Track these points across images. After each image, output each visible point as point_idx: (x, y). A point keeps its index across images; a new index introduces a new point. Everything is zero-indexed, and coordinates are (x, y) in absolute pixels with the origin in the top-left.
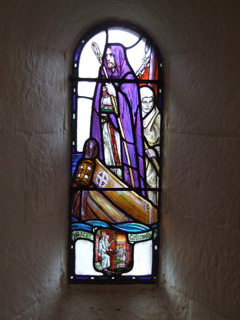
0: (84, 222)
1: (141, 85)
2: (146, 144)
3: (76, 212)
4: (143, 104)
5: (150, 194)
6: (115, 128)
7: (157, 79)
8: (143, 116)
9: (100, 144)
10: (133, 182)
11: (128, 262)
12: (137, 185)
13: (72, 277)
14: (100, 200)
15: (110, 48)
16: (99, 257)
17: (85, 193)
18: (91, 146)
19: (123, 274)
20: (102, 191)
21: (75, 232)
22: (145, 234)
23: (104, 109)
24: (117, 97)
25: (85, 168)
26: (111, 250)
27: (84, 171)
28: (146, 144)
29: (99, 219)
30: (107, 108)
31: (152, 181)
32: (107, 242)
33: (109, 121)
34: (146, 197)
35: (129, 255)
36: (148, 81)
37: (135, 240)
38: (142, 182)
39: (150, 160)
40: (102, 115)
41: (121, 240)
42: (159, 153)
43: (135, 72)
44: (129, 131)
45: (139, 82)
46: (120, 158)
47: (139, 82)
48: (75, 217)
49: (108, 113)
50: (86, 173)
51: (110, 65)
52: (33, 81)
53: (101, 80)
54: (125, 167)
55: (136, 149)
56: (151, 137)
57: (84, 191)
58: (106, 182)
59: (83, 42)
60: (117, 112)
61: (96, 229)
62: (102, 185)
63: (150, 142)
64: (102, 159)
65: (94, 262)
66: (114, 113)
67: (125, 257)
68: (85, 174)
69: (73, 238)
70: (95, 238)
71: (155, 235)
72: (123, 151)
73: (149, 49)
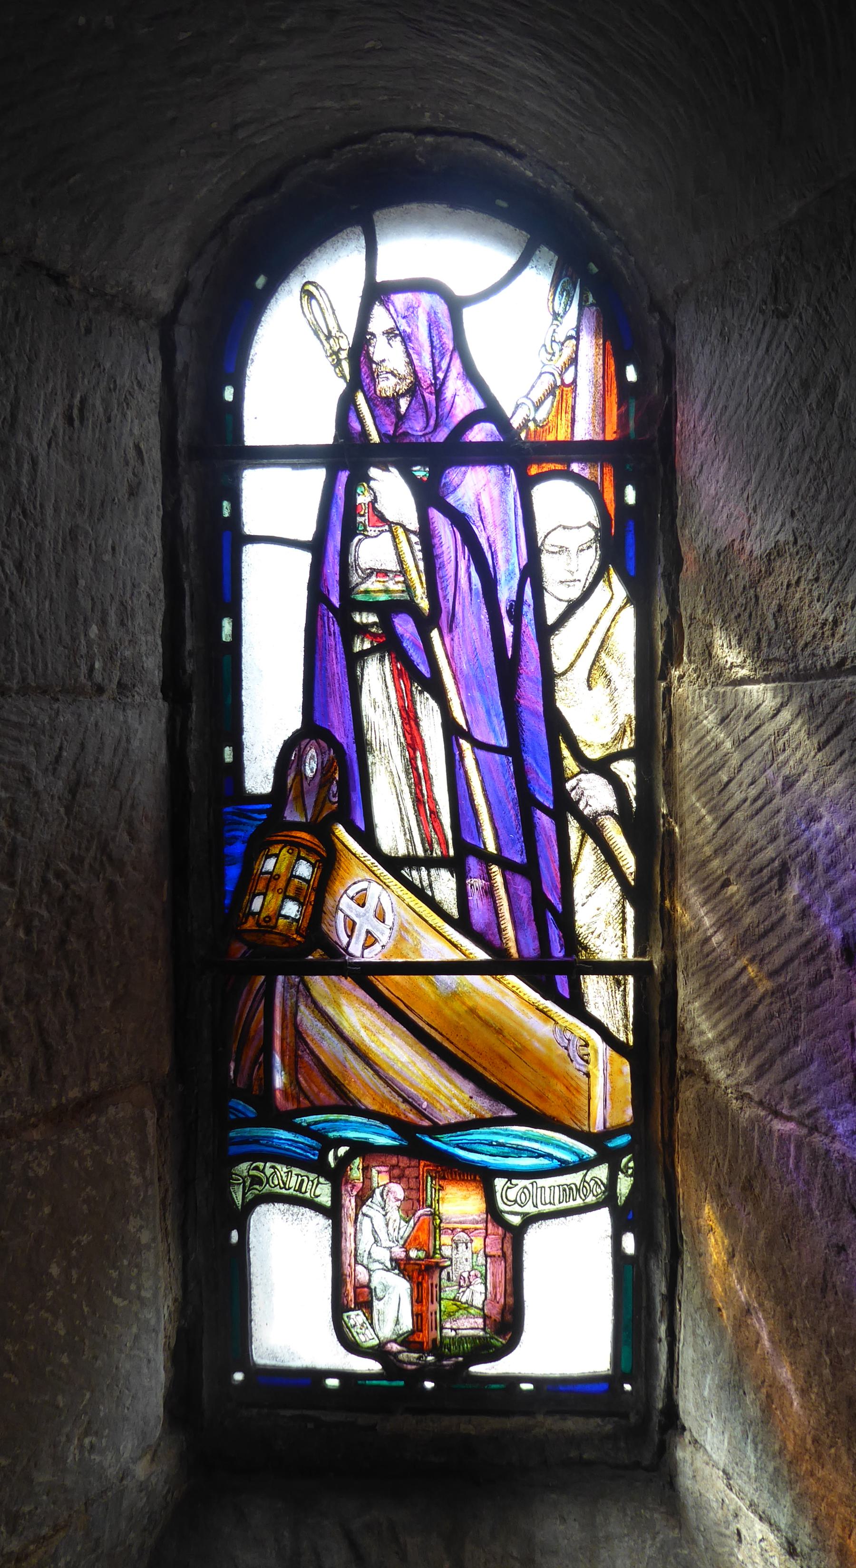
0: (286, 1121)
2: (566, 752)
3: (250, 1075)
5: (597, 992)
6: (418, 678)
7: (610, 436)
8: (551, 619)
10: (510, 932)
11: (494, 1311)
12: (532, 949)
13: (239, 1376)
14: (357, 1016)
15: (385, 304)
16: (358, 1287)
18: (311, 768)
20: (365, 976)
21: (244, 1167)
22: (575, 1178)
23: (367, 592)
24: (426, 534)
25: (283, 869)
27: (281, 884)
28: (566, 752)
30: (379, 586)
33: (389, 645)
34: (575, 1005)
35: (501, 1278)
37: (529, 1209)
38: (554, 933)
39: (592, 828)
41: (460, 1204)
42: (632, 792)
43: (508, 411)
44: (482, 690)
45: (524, 457)
47: (524, 457)
49: (386, 610)
51: (386, 386)
53: (347, 458)
54: (473, 863)
56: (597, 711)
57: (280, 978)
58: (383, 933)
59: (261, 282)
60: (424, 604)
61: (342, 1151)
62: (365, 947)
64: (361, 825)
65: (339, 1308)
66: (408, 606)
68: (286, 897)
70: (336, 1196)
71: (624, 1185)
72: (461, 783)
73: (570, 298)
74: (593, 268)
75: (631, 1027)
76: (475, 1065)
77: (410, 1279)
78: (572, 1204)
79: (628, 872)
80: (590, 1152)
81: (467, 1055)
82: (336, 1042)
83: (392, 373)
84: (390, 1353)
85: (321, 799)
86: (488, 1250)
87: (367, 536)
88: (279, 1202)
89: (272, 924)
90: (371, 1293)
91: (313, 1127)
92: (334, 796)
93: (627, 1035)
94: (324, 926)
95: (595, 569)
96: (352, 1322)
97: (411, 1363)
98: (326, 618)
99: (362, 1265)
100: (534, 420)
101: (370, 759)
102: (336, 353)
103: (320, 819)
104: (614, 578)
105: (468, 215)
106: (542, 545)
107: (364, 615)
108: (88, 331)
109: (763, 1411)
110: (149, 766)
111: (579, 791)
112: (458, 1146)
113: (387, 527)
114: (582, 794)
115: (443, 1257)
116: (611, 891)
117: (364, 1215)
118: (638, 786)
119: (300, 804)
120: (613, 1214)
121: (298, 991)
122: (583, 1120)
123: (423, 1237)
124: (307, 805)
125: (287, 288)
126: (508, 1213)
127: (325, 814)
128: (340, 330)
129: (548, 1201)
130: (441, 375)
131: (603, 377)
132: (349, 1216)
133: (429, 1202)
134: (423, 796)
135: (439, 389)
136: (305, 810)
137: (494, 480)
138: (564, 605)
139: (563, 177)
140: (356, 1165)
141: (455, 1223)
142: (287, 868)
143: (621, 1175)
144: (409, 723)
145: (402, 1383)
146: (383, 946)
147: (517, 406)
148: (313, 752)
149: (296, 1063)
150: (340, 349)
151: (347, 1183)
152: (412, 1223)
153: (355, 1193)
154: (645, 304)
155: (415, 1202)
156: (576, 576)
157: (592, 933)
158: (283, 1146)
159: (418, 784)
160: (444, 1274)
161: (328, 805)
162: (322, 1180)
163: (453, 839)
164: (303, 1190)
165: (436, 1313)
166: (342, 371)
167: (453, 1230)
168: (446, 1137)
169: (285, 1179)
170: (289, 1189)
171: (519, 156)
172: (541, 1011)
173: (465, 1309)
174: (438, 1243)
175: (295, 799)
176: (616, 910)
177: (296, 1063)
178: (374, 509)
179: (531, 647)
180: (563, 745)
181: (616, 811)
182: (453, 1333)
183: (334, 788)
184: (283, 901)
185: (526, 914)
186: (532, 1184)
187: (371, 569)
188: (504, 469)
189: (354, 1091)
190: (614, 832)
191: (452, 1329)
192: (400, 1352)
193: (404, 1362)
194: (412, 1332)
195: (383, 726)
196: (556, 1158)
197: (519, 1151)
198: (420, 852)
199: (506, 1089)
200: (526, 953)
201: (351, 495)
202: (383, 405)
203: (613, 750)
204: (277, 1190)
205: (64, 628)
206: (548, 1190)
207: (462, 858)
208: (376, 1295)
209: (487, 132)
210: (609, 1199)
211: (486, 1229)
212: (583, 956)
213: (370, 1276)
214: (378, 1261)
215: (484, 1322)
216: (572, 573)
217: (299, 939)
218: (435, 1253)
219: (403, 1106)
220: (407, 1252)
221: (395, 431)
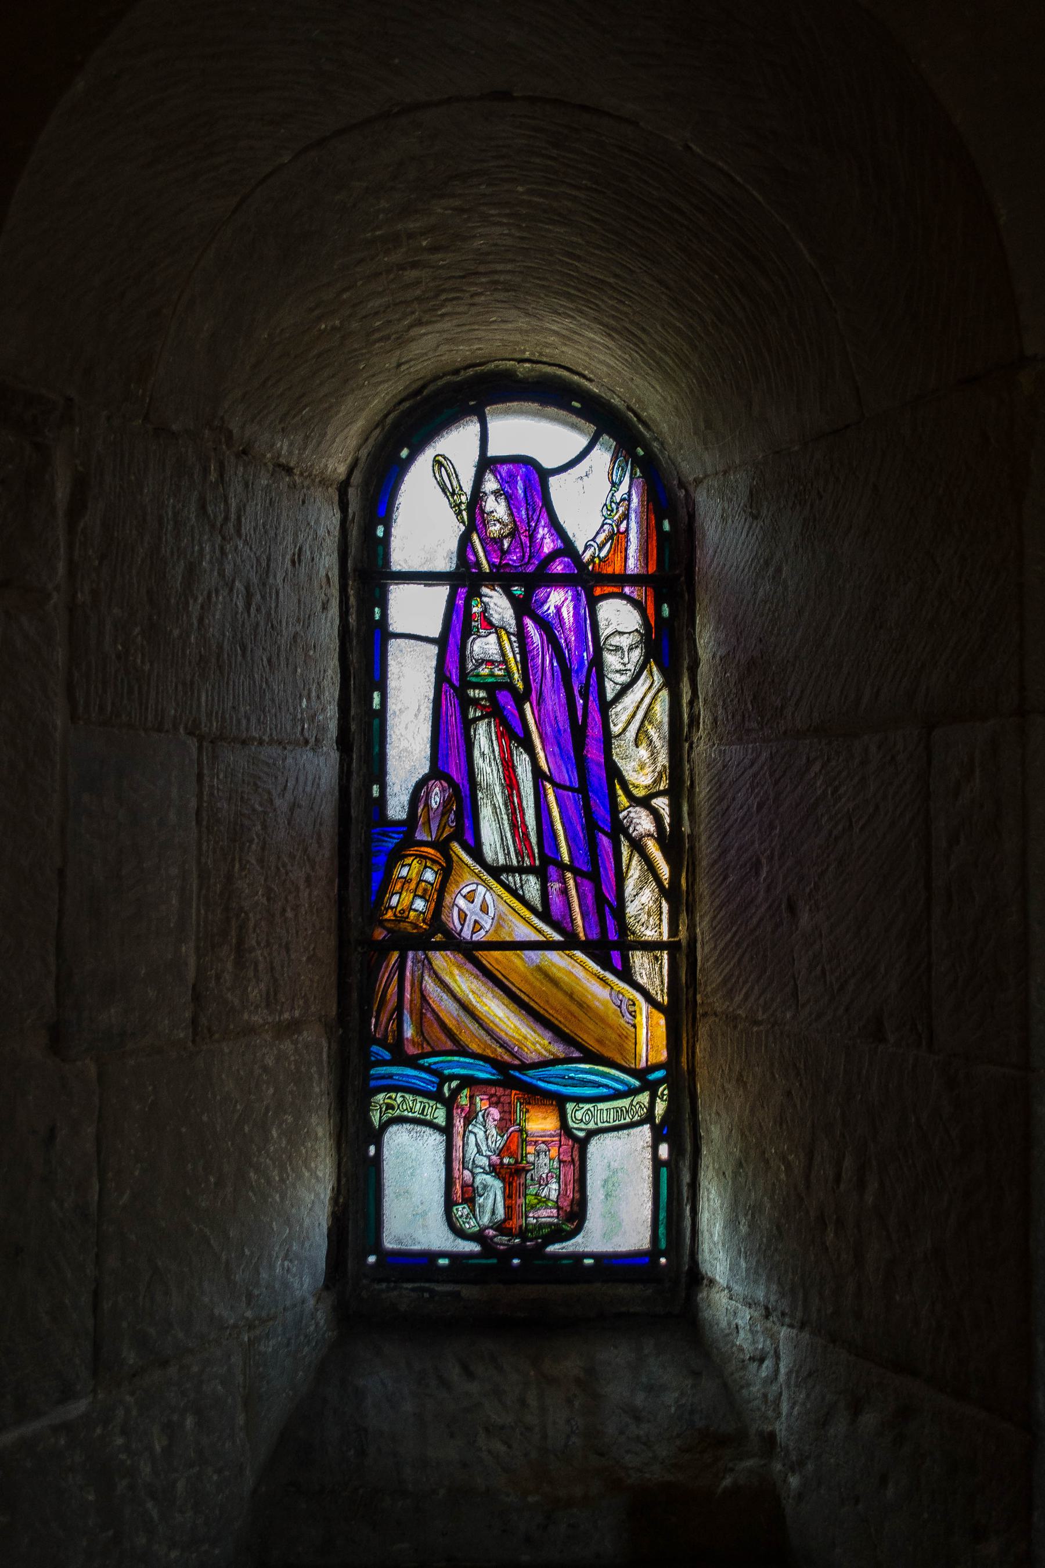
0: (412, 1062)
2: (620, 792)
4: (605, 654)
5: (641, 963)
11: (565, 1204)
13: (372, 1259)
15: (495, 472)
16: (465, 1185)
18: (435, 801)
19: (551, 1249)
20: (470, 952)
21: (380, 1097)
22: (625, 1103)
23: (478, 676)
25: (414, 874)
27: (413, 886)
28: (620, 792)
30: (486, 672)
31: (644, 918)
32: (494, 1132)
33: (494, 712)
34: (626, 974)
35: (570, 1177)
37: (592, 1126)
38: (610, 922)
39: (638, 846)
40: (471, 693)
41: (541, 1123)
42: (667, 820)
43: (581, 549)
45: (590, 582)
46: (534, 839)
48: (383, 1043)
49: (491, 688)
50: (420, 893)
51: (494, 530)
52: (228, 569)
53: (464, 580)
54: (552, 870)
58: (487, 923)
59: (404, 453)
60: (520, 685)
61: (454, 1084)
62: (473, 933)
63: (637, 783)
65: (449, 1204)
66: (510, 686)
67: (555, 1186)
69: (376, 1118)
70: (449, 1118)
71: (660, 1107)
74: (640, 451)
75: (666, 990)
77: (503, 1180)
78: (623, 1121)
80: (637, 1083)
83: (498, 521)
84: (487, 1237)
87: (479, 636)
89: (405, 915)
91: (433, 1067)
97: (504, 1245)
101: (480, 795)
102: (459, 505)
104: (655, 669)
105: (551, 410)
107: (477, 691)
108: (304, 502)
109: (749, 1226)
110: (330, 797)
112: (540, 1079)
115: (528, 1163)
117: (470, 1132)
118: (670, 816)
121: (423, 965)
123: (513, 1147)
126: (577, 1129)
127: (445, 835)
132: (459, 1133)
137: (570, 598)
138: (618, 687)
139: (619, 397)
142: (417, 874)
145: (495, 1261)
147: (587, 547)
149: (421, 1019)
150: (461, 503)
154: (675, 482)
156: (628, 667)
160: (529, 1176)
162: (439, 1105)
166: (462, 518)
167: (536, 1142)
168: (531, 1072)
171: (590, 380)
175: (423, 824)
177: (421, 1019)
179: (595, 716)
180: (618, 787)
183: (452, 816)
185: (590, 909)
190: (653, 848)
191: (534, 1218)
192: (495, 1236)
193: (497, 1244)
194: (504, 1221)
195: (489, 770)
197: (585, 1083)
198: (515, 863)
200: (590, 937)
201: (468, 606)
202: (492, 544)
204: (406, 1113)
205: (290, 701)
207: (546, 866)
209: (568, 365)
210: (649, 1118)
211: (560, 1141)
214: (481, 1167)
216: (624, 664)
219: (499, 1050)
220: (502, 1159)
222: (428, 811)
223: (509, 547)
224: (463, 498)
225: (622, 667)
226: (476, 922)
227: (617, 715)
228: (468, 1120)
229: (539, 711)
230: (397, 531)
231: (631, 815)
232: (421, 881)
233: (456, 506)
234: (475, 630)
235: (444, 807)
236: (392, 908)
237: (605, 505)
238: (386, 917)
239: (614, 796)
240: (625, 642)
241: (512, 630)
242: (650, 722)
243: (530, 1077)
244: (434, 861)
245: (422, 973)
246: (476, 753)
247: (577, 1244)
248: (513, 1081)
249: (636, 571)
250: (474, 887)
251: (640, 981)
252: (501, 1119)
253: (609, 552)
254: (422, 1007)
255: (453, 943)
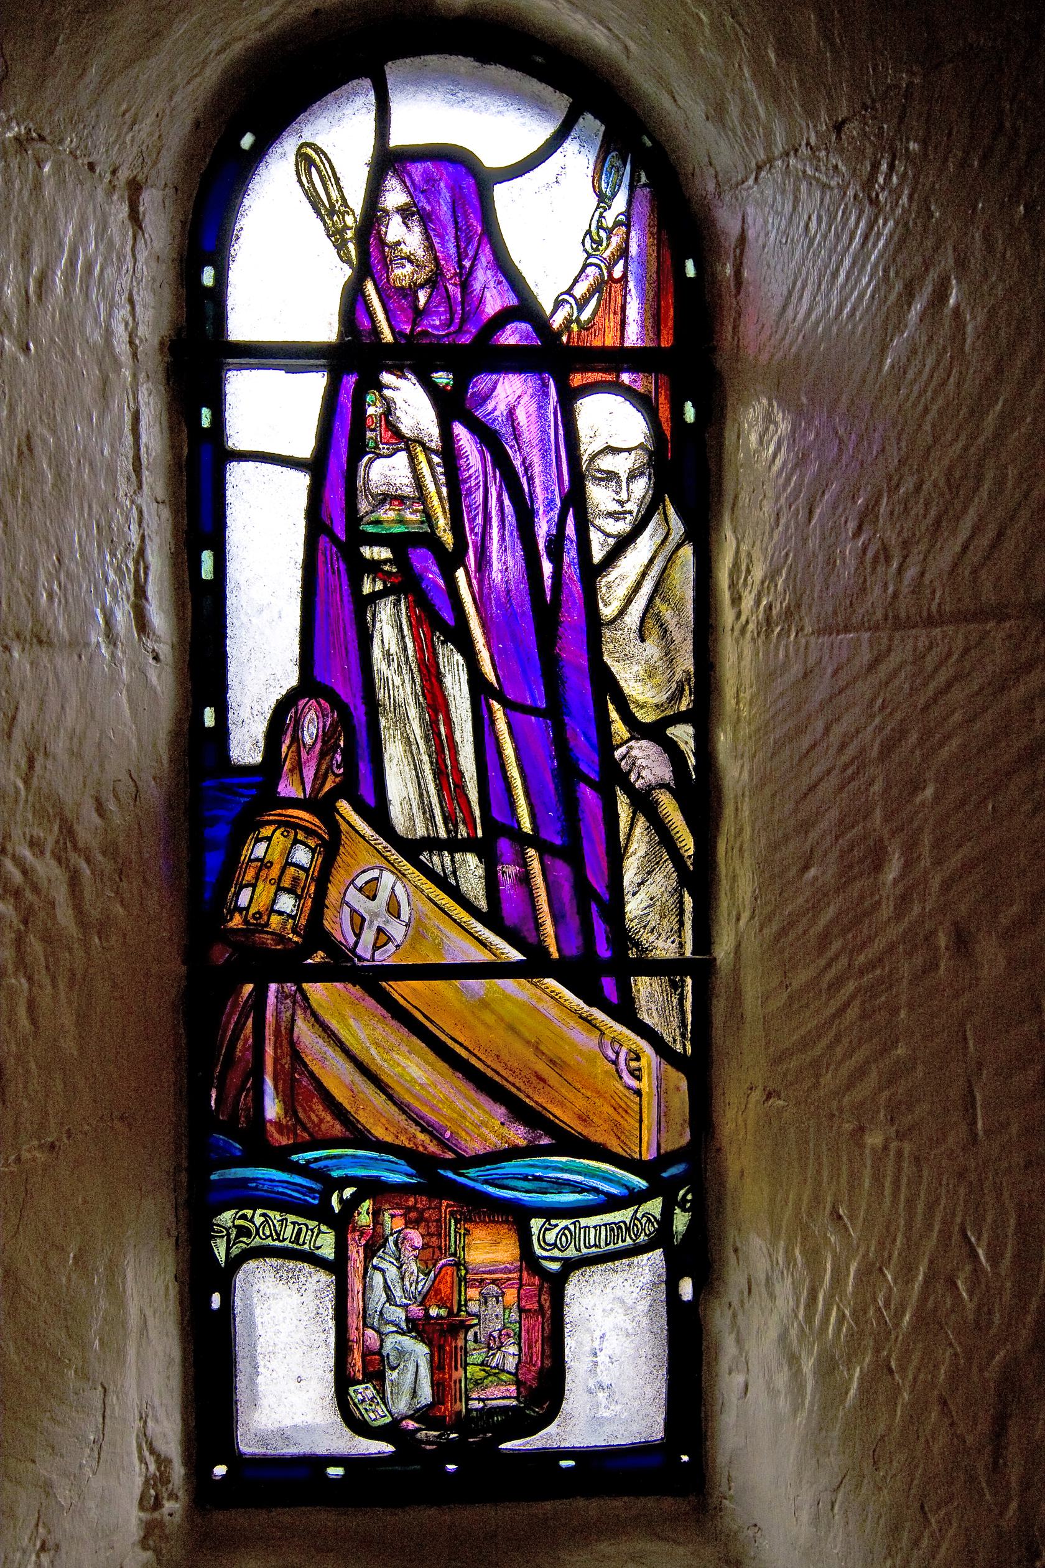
0: (280, 1159)
1: (577, 379)
2: (614, 715)
7: (666, 342)
8: (598, 555)
9: (359, 713)
10: (549, 928)
11: (530, 1376)
13: (220, 1470)
17: (281, 996)
20: (373, 981)
21: (227, 1217)
22: (624, 1215)
23: (377, 522)
24: (449, 452)
25: (275, 855)
26: (434, 1312)
27: (275, 873)
28: (614, 715)
29: (360, 1138)
30: (392, 515)
33: (405, 584)
35: (537, 1335)
36: (618, 358)
37: (571, 1253)
38: (600, 927)
39: (644, 803)
40: (366, 552)
41: (489, 1250)
42: (692, 761)
43: (548, 308)
46: (473, 795)
47: (563, 363)
50: (286, 883)
51: (402, 274)
53: (352, 361)
54: (504, 845)
55: (561, 743)
57: (273, 987)
58: (397, 930)
59: (247, 141)
60: (448, 539)
61: (348, 1192)
62: (376, 947)
63: (641, 698)
64: (371, 801)
65: (343, 1381)
66: (430, 540)
67: (513, 1349)
68: (279, 889)
69: (220, 1250)
70: (341, 1247)
71: (681, 1221)
76: (508, 1086)
77: (429, 1344)
78: (620, 1244)
79: (686, 854)
80: (643, 1184)
81: (498, 1073)
82: (341, 1062)
85: (322, 772)
86: (523, 1303)
87: (380, 456)
88: (270, 1256)
90: (382, 1361)
92: (338, 767)
93: (684, 1046)
94: (325, 922)
95: (648, 499)
96: (360, 1397)
98: (328, 553)
99: (373, 1328)
100: (578, 321)
101: (383, 722)
103: (320, 795)
104: (671, 511)
105: (498, 72)
106: (587, 469)
107: (376, 549)
111: (630, 761)
112: (486, 1182)
113: (402, 445)
114: (634, 764)
116: (663, 881)
117: (375, 1268)
119: (296, 777)
120: (666, 1254)
121: (294, 1002)
122: (633, 1147)
123: (445, 1290)
124: (306, 780)
125: (279, 150)
126: (545, 1258)
127: (326, 788)
128: (347, 206)
129: (592, 1243)
130: (467, 264)
131: (658, 273)
133: (452, 1250)
134: (447, 767)
135: (466, 280)
136: (303, 783)
137: (530, 391)
138: (611, 541)
140: (365, 1209)
141: (484, 1273)
143: (677, 1211)
144: (430, 680)
146: (398, 946)
147: (558, 304)
148: (312, 714)
149: (292, 1088)
151: (354, 1231)
152: (432, 1274)
153: (363, 1242)
155: (436, 1250)
156: (628, 507)
157: (645, 927)
158: (276, 1189)
159: (440, 751)
161: (331, 778)
162: (323, 1228)
163: (482, 817)
164: (301, 1241)
165: (460, 1381)
167: (483, 1280)
168: (472, 1172)
169: (278, 1229)
170: (284, 1240)
172: (585, 1019)
173: (495, 1375)
174: (463, 1298)
175: (291, 771)
176: (672, 900)
177: (292, 1088)
178: (388, 422)
180: (611, 707)
181: (672, 783)
182: (481, 1404)
183: (339, 758)
184: (276, 894)
186: (574, 1223)
187: (383, 494)
188: (543, 380)
189: (363, 1120)
191: (479, 1399)
192: (419, 1430)
193: (421, 1441)
194: (429, 1406)
195: (397, 681)
196: (603, 1192)
197: (561, 1185)
198: (443, 834)
199: (544, 1112)
202: (398, 298)
203: (669, 712)
204: (269, 1241)
206: (592, 1231)
208: (389, 1363)
210: (662, 1237)
211: (520, 1278)
212: (632, 954)
213: (382, 1341)
214: (392, 1323)
215: (518, 1389)
216: (621, 503)
217: (296, 939)
218: (459, 1310)
219: (421, 1136)
220: (427, 1310)
221: (412, 330)
222: (298, 748)
223: (427, 303)
224: (349, 220)
225: (618, 508)
226: (380, 930)
227: (609, 588)
228: (371, 1251)
229: (481, 582)
230: (235, 274)
231: (634, 753)
232: (288, 864)
233: (336, 235)
234: (371, 444)
235: (324, 742)
236: (240, 910)
237: (589, 232)
238: (231, 924)
239: (605, 723)
240: (621, 464)
241: (433, 445)
242: (664, 600)
243: (471, 1177)
244: (310, 832)
245: (293, 1015)
246: (377, 653)
247: (549, 1437)
248: (442, 1185)
249: (639, 344)
250: (375, 873)
251: (647, 1020)
252: (425, 1246)
253: (595, 312)
254: (293, 1069)
255: (343, 967)
